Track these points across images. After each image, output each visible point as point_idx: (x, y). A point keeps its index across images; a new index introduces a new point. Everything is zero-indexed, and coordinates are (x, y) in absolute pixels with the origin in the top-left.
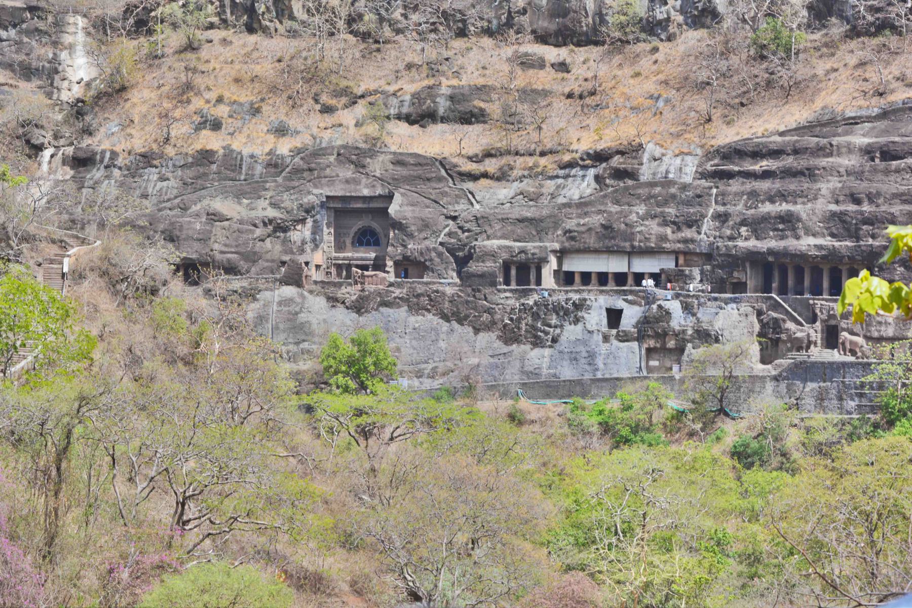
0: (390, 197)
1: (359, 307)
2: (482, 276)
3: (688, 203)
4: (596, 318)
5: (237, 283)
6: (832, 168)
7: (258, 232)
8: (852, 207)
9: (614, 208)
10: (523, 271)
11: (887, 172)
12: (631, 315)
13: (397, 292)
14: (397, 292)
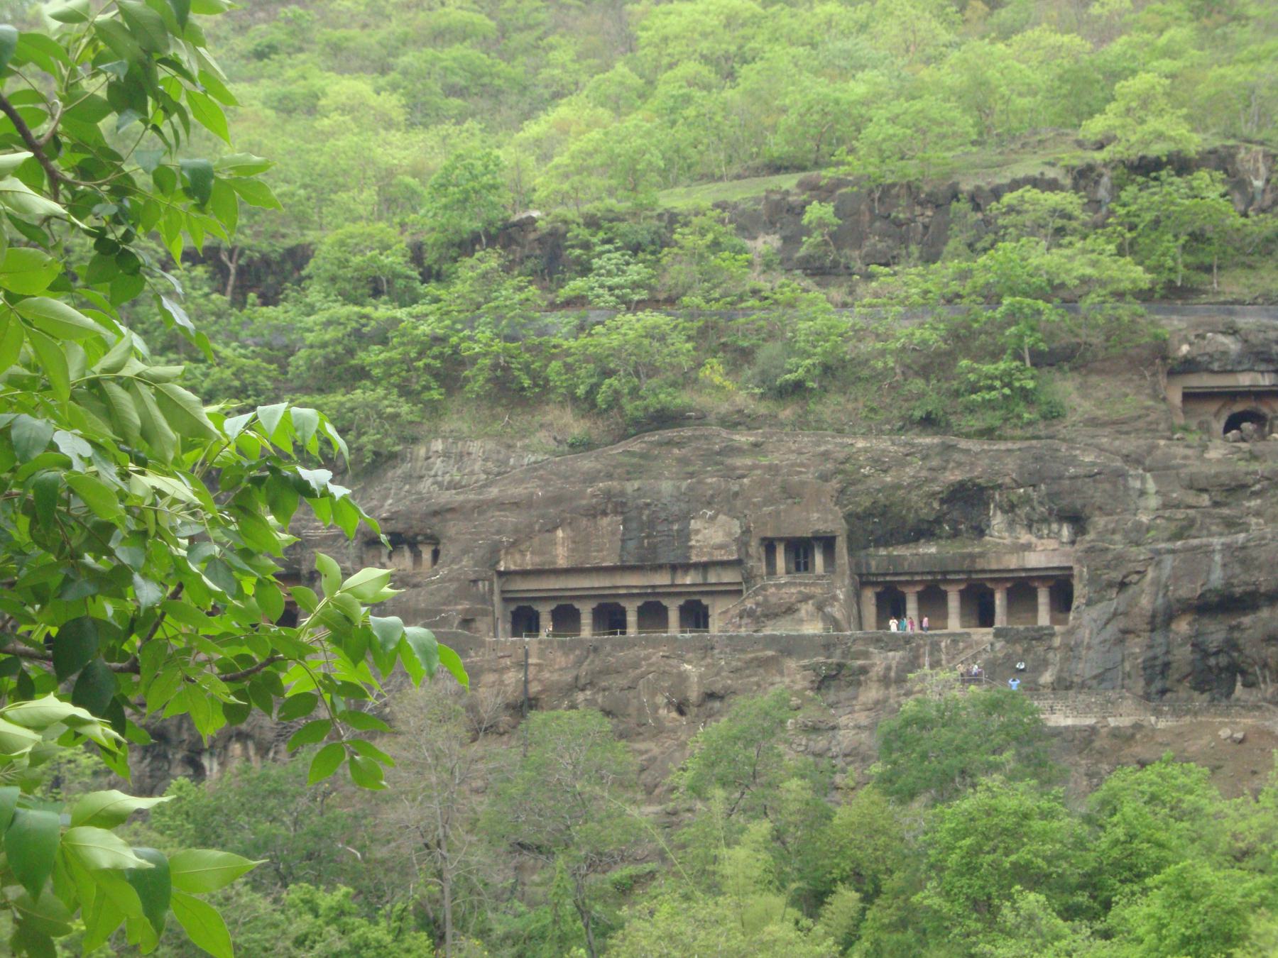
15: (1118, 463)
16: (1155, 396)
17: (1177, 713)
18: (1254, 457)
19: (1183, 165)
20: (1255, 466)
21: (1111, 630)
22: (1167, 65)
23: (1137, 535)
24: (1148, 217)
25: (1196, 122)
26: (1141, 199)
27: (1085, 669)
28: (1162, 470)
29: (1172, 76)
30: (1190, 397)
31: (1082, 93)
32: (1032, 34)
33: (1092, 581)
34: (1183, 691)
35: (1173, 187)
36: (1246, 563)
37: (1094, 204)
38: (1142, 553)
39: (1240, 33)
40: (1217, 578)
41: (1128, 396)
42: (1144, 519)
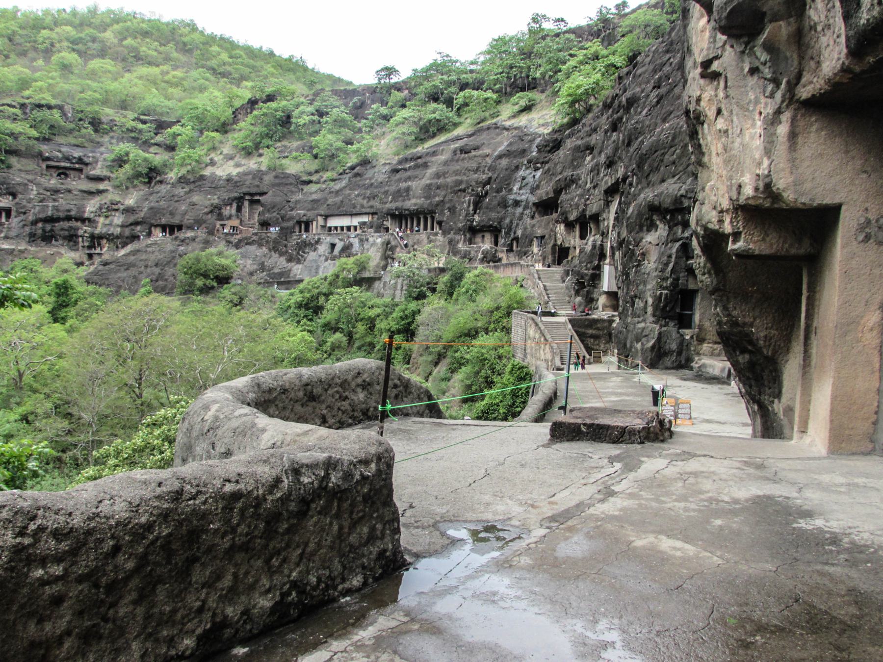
0: (265, 193)
1: (237, 246)
2: (287, 228)
3: (376, 187)
4: (323, 249)
5: (190, 234)
6: (436, 161)
7: (206, 210)
8: (435, 181)
9: (348, 192)
10: (307, 225)
11: (457, 161)
12: (339, 246)
13: (254, 238)
14: (254, 238)
15: (26, 182)
16: (38, 165)
17: (37, 246)
18: (62, 184)
19: (50, 107)
20: (63, 187)
21: (21, 224)
22: (51, 81)
23: (30, 201)
24: (40, 119)
25: (54, 97)
26: (38, 114)
27: (13, 233)
28: (38, 185)
29: (50, 85)
30: (48, 167)
31: (24, 84)
32: (16, 67)
33: (17, 211)
34: (39, 241)
35: (46, 113)
36: (58, 210)
37: (25, 113)
38: (31, 205)
39: (71, 76)
40: (50, 213)
41: (31, 165)
42: (32, 197)
